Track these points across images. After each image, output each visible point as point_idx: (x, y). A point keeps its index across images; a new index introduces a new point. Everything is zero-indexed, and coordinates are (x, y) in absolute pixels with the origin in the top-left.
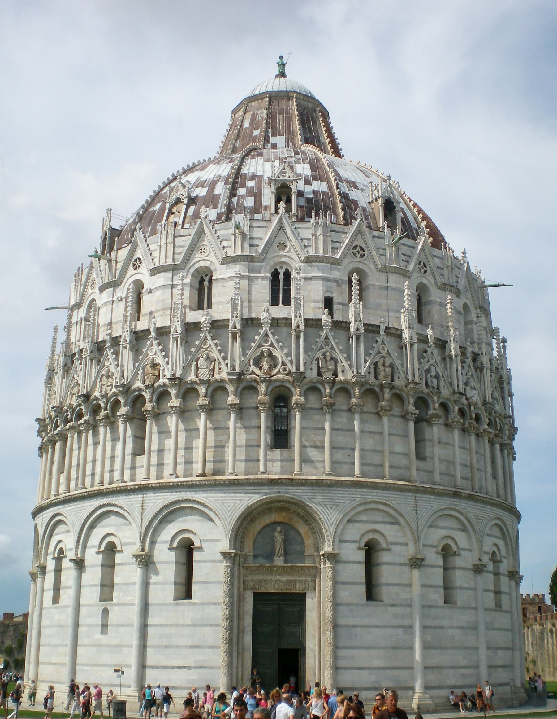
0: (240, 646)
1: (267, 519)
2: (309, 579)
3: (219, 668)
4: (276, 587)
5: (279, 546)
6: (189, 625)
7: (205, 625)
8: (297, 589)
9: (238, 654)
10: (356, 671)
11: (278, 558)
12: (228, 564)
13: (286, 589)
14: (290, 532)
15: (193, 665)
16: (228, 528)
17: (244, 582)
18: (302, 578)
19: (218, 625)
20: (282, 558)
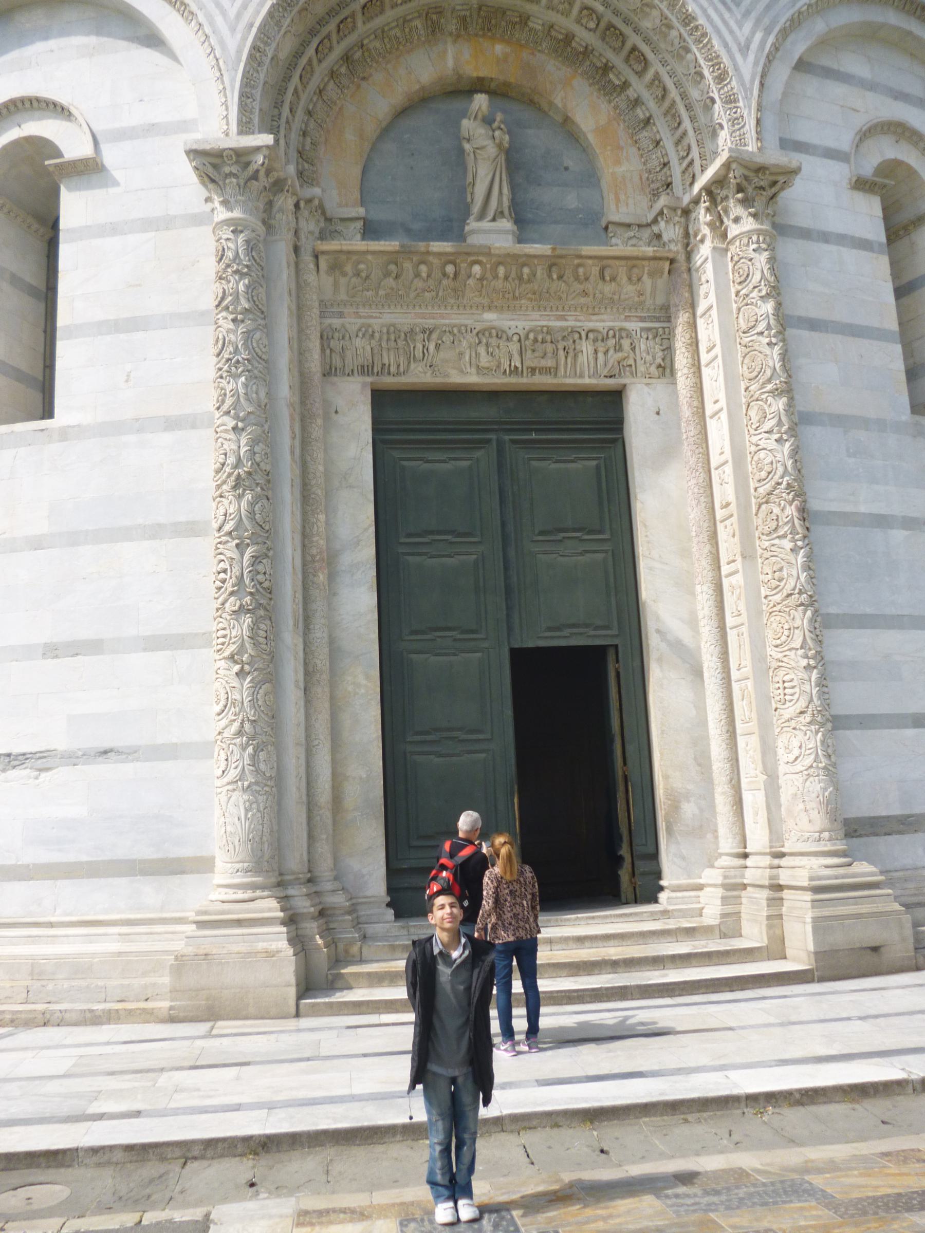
0: (319, 633)
1: (425, 67)
2: (634, 326)
3: (203, 751)
4: (485, 360)
5: (485, 174)
6: (37, 544)
7: (126, 534)
8: (585, 371)
9: (309, 673)
10: (910, 732)
11: (485, 224)
12: (237, 214)
13: (533, 370)
14: (530, 132)
15: (61, 744)
16: (232, 44)
17: (325, 338)
18: (603, 322)
19: (192, 529)
20: (506, 224)
